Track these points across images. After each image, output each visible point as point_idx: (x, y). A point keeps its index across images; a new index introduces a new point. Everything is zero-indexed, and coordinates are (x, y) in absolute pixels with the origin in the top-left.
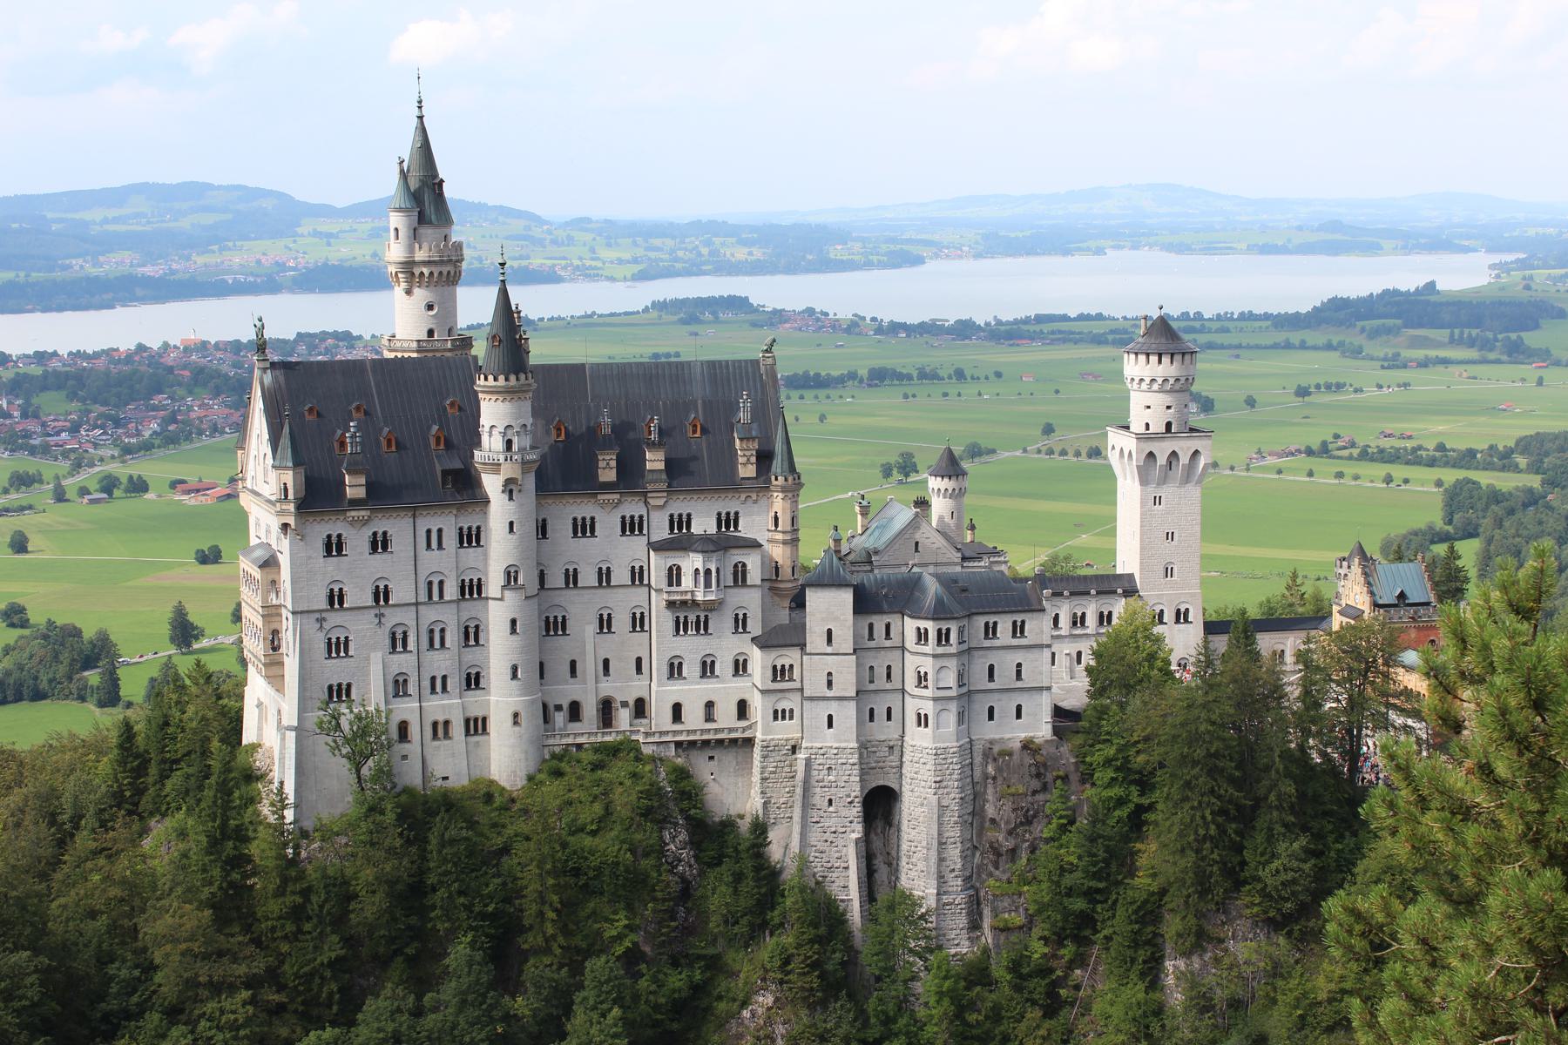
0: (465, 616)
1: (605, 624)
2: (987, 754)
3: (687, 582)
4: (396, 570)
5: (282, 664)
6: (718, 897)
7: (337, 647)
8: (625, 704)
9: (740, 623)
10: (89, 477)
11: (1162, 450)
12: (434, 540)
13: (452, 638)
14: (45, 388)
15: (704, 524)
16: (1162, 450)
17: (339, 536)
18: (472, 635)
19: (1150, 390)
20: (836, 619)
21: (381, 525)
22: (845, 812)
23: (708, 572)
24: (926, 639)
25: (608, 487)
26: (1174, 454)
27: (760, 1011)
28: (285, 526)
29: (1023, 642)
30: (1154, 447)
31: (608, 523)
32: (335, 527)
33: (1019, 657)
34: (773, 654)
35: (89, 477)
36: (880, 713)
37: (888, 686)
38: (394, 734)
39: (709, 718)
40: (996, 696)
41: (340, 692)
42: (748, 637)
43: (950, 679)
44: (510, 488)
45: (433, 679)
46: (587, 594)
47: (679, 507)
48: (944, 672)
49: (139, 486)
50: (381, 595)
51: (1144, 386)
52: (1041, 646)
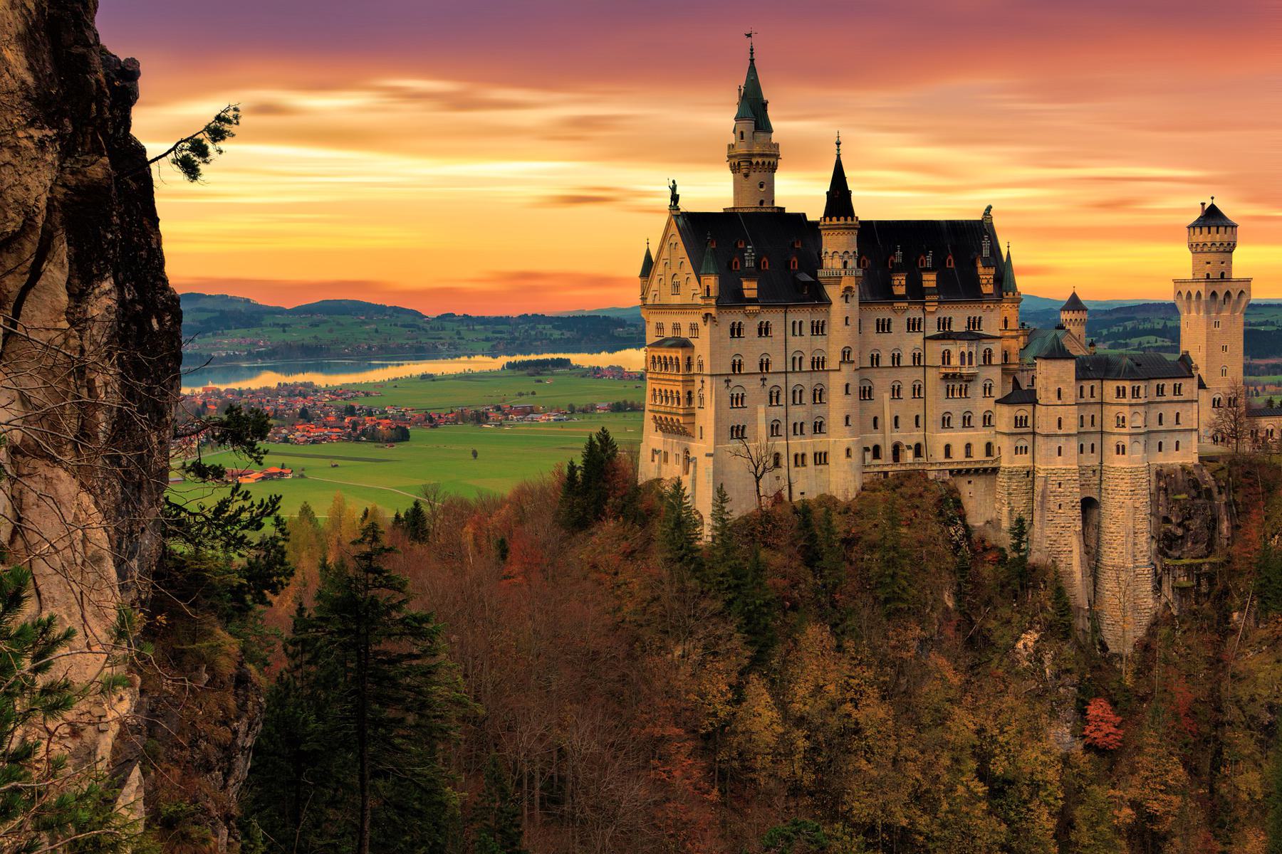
1: (896, 392)
2: (1159, 474)
3: (955, 361)
4: (773, 348)
7: (737, 400)
8: (909, 447)
9: (987, 390)
12: (797, 328)
13: (807, 397)
15: (959, 326)
16: (1221, 289)
18: (819, 395)
19: (1210, 252)
20: (1064, 381)
22: (1070, 513)
23: (970, 354)
25: (901, 298)
26: (1228, 294)
27: (1030, 644)
29: (1180, 398)
31: (899, 323)
32: (737, 317)
33: (1178, 408)
34: (1016, 408)
36: (1087, 448)
37: (1092, 429)
38: (772, 462)
39: (968, 455)
40: (1163, 435)
41: (738, 432)
42: (992, 400)
43: (1139, 421)
46: (885, 372)
50: (765, 365)
51: (1206, 249)
52: (1192, 401)
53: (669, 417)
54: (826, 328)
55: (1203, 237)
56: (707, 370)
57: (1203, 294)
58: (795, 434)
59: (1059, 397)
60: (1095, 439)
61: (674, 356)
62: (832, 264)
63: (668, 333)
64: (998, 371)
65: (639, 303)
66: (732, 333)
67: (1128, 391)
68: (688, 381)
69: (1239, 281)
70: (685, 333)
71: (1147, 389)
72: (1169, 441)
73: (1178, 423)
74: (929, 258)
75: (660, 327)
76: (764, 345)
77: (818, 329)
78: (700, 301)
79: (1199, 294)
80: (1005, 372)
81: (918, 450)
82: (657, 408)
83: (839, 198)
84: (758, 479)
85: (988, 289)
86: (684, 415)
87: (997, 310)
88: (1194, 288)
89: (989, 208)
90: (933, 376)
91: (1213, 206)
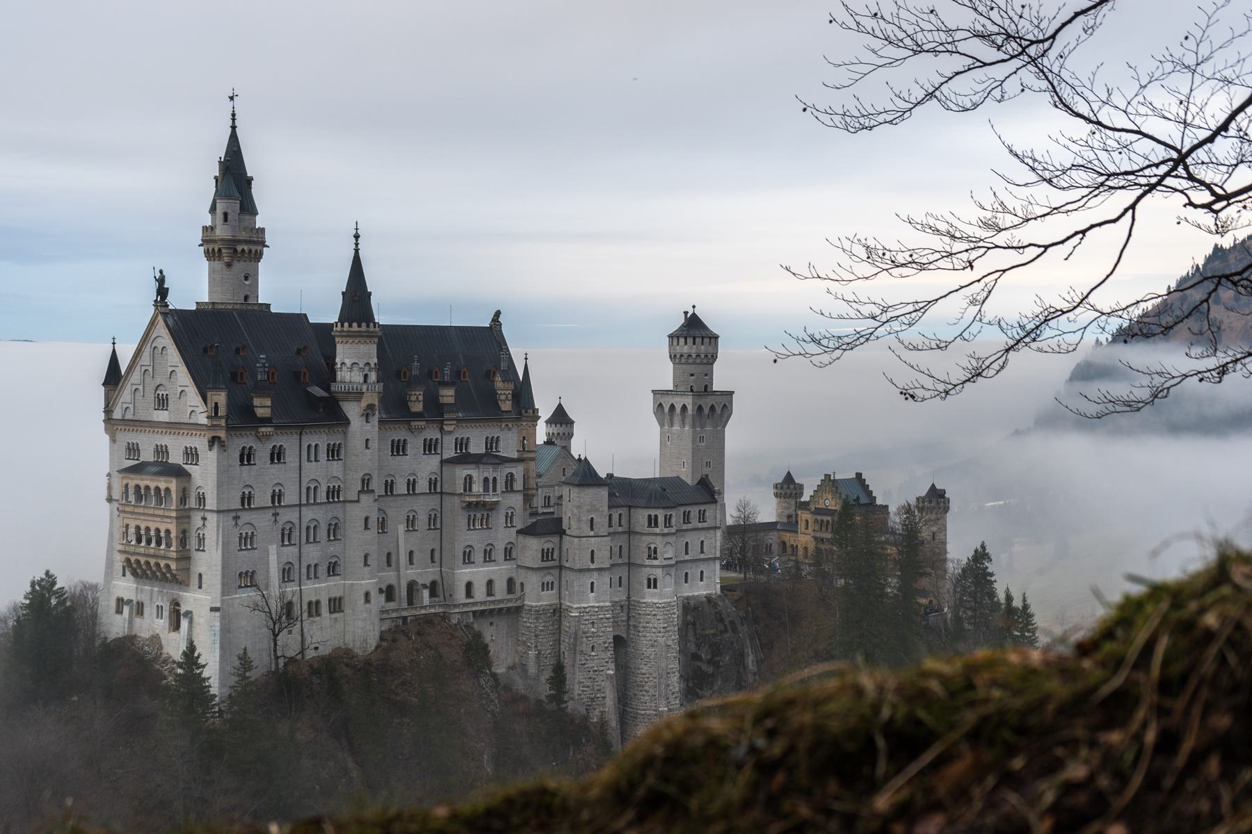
0: (330, 515)
1: (411, 522)
3: (477, 488)
4: (284, 476)
5: (188, 558)
7: (247, 541)
11: (707, 402)
12: (312, 453)
13: (322, 533)
15: (477, 447)
16: (707, 402)
17: (251, 448)
18: (334, 530)
19: (694, 363)
20: (596, 510)
21: (280, 440)
22: (603, 655)
23: (495, 479)
24: (656, 525)
25: (418, 416)
26: (712, 408)
28: (213, 441)
29: (705, 525)
30: (702, 402)
32: (248, 441)
33: (702, 536)
34: (543, 540)
39: (490, 593)
40: (689, 565)
41: (248, 579)
44: (367, 414)
45: (309, 566)
47: (462, 433)
48: (669, 547)
50: (277, 497)
51: (691, 361)
53: (152, 562)
54: (342, 452)
55: (684, 348)
56: (211, 503)
57: (690, 408)
58: (308, 578)
59: (592, 529)
60: (623, 572)
61: (162, 486)
63: (147, 455)
64: (520, 497)
65: (102, 416)
66: (242, 460)
67: (661, 520)
68: (184, 516)
69: (723, 393)
70: (176, 458)
71: (677, 515)
72: (694, 571)
73: (702, 552)
74: (447, 371)
75: (133, 450)
76: (275, 474)
77: (334, 452)
78: (203, 420)
79: (684, 408)
80: (528, 498)
81: (433, 588)
82: (132, 549)
84: (275, 636)
85: (506, 406)
86: (177, 560)
87: (515, 429)
88: (679, 402)
89: (498, 314)
90: (453, 504)
91: (694, 314)
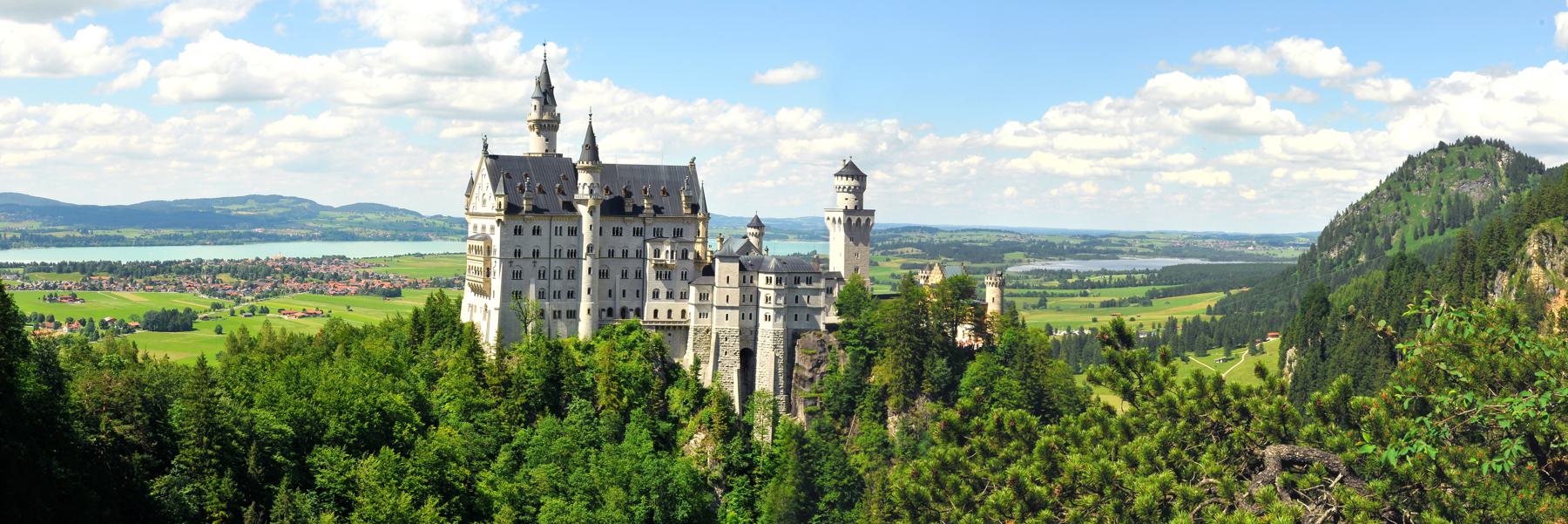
1: (624, 275)
3: (663, 257)
4: (540, 242)
6: (676, 395)
7: (517, 275)
10: (244, 306)
12: (558, 231)
13: (564, 275)
14: (220, 272)
15: (668, 231)
25: (629, 214)
32: (519, 223)
35: (244, 306)
43: (781, 301)
44: (591, 212)
49: (265, 311)
50: (536, 254)
62: (583, 192)
63: (479, 231)
68: (487, 260)
70: (488, 231)
83: (591, 148)
